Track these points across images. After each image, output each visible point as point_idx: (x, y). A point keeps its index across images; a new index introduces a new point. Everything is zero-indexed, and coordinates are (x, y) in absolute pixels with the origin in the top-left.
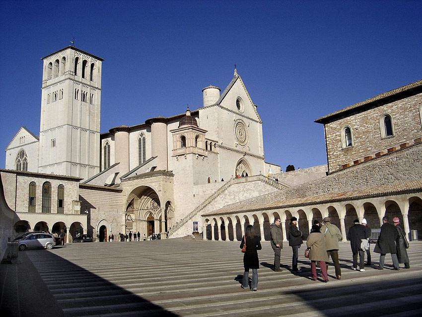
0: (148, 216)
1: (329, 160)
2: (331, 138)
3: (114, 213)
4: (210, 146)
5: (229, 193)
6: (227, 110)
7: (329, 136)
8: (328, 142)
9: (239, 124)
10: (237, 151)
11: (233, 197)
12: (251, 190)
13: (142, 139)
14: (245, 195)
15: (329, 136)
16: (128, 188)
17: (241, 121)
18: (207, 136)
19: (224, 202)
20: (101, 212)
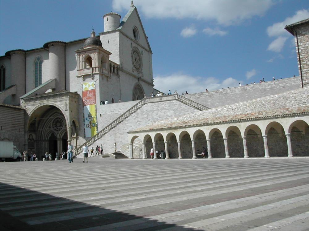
0: (50, 135)
1: (302, 70)
2: (303, 46)
3: (17, 132)
4: (114, 69)
5: (142, 112)
6: (127, 36)
7: (302, 44)
8: (300, 51)
9: (135, 52)
10: (134, 76)
11: (145, 116)
12: (166, 109)
13: (39, 62)
14: (159, 114)
15: (302, 44)
16: (31, 108)
19: (136, 121)
20: (4, 131)
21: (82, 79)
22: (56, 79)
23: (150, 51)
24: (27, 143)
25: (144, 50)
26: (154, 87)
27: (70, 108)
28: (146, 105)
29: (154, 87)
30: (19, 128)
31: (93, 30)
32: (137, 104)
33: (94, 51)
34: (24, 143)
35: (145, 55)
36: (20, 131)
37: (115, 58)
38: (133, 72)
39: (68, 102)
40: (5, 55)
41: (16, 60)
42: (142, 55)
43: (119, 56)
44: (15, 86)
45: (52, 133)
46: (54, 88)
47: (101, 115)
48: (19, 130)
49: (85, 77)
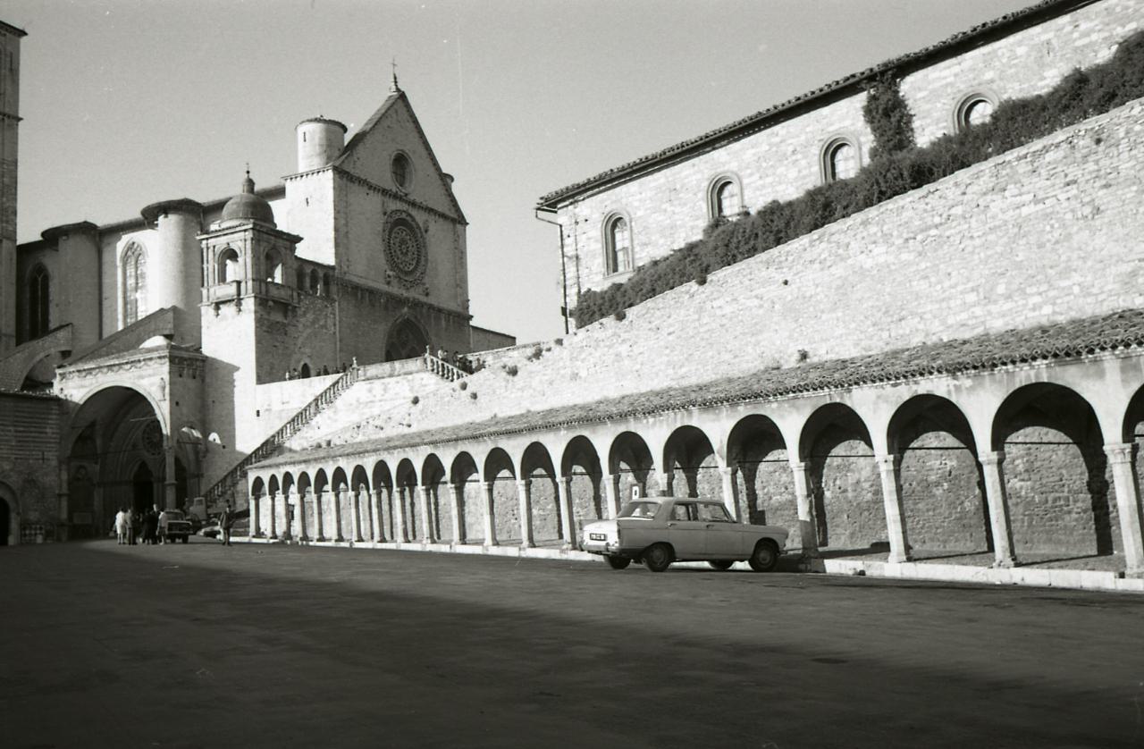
17: (404, 215)
18: (302, 251)
21: (211, 311)
22: (174, 309)
23: (459, 220)
24: (65, 490)
25: (432, 218)
26: (472, 323)
27: (171, 394)
28: (356, 384)
29: (472, 323)
30: (39, 451)
31: (248, 172)
32: (337, 382)
33: (242, 233)
34: (57, 492)
35: (436, 233)
36: (43, 459)
37: (318, 247)
38: (389, 283)
39: (167, 377)
40: (41, 239)
41: (73, 252)
42: (426, 231)
43: (332, 244)
44: (70, 328)
45: (139, 463)
46: (167, 332)
47: (258, 412)
48: (40, 457)
49: (217, 306)
